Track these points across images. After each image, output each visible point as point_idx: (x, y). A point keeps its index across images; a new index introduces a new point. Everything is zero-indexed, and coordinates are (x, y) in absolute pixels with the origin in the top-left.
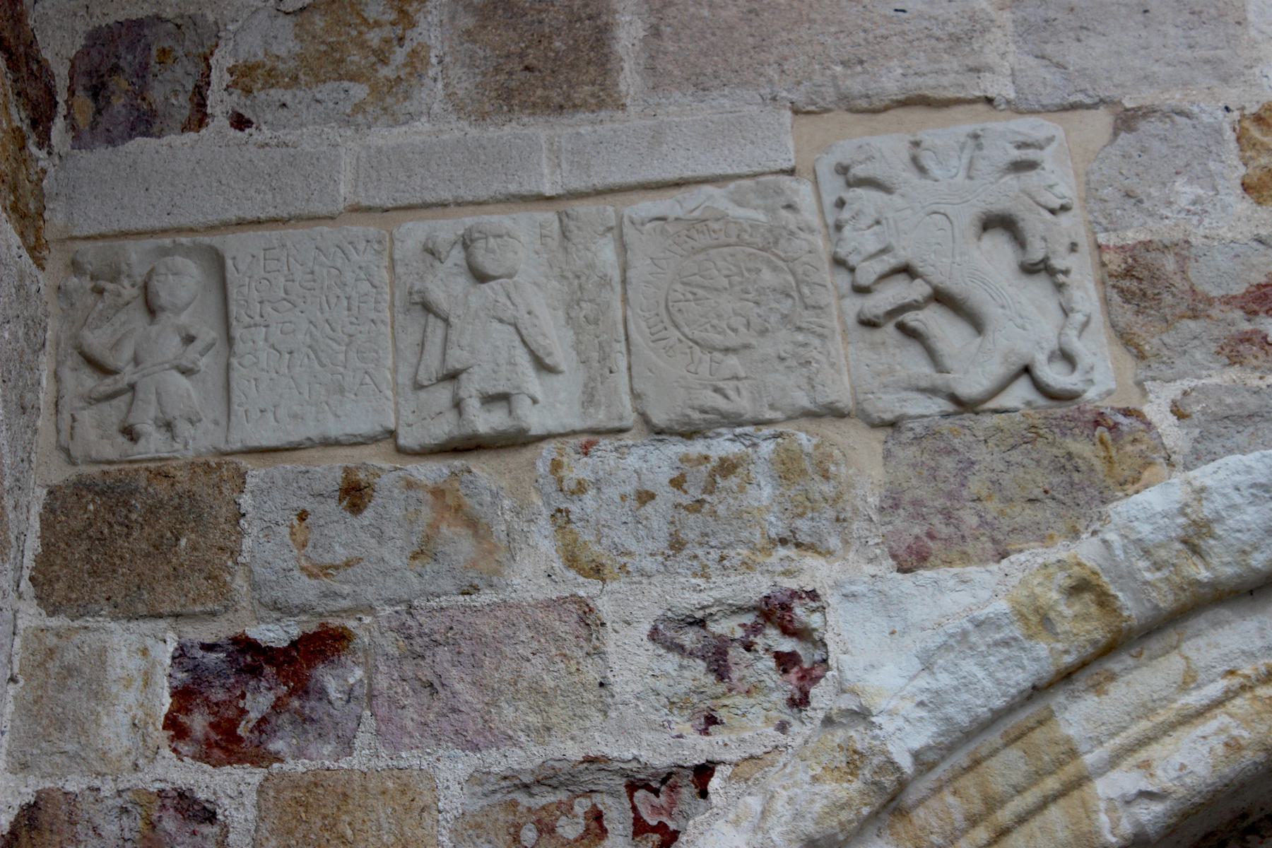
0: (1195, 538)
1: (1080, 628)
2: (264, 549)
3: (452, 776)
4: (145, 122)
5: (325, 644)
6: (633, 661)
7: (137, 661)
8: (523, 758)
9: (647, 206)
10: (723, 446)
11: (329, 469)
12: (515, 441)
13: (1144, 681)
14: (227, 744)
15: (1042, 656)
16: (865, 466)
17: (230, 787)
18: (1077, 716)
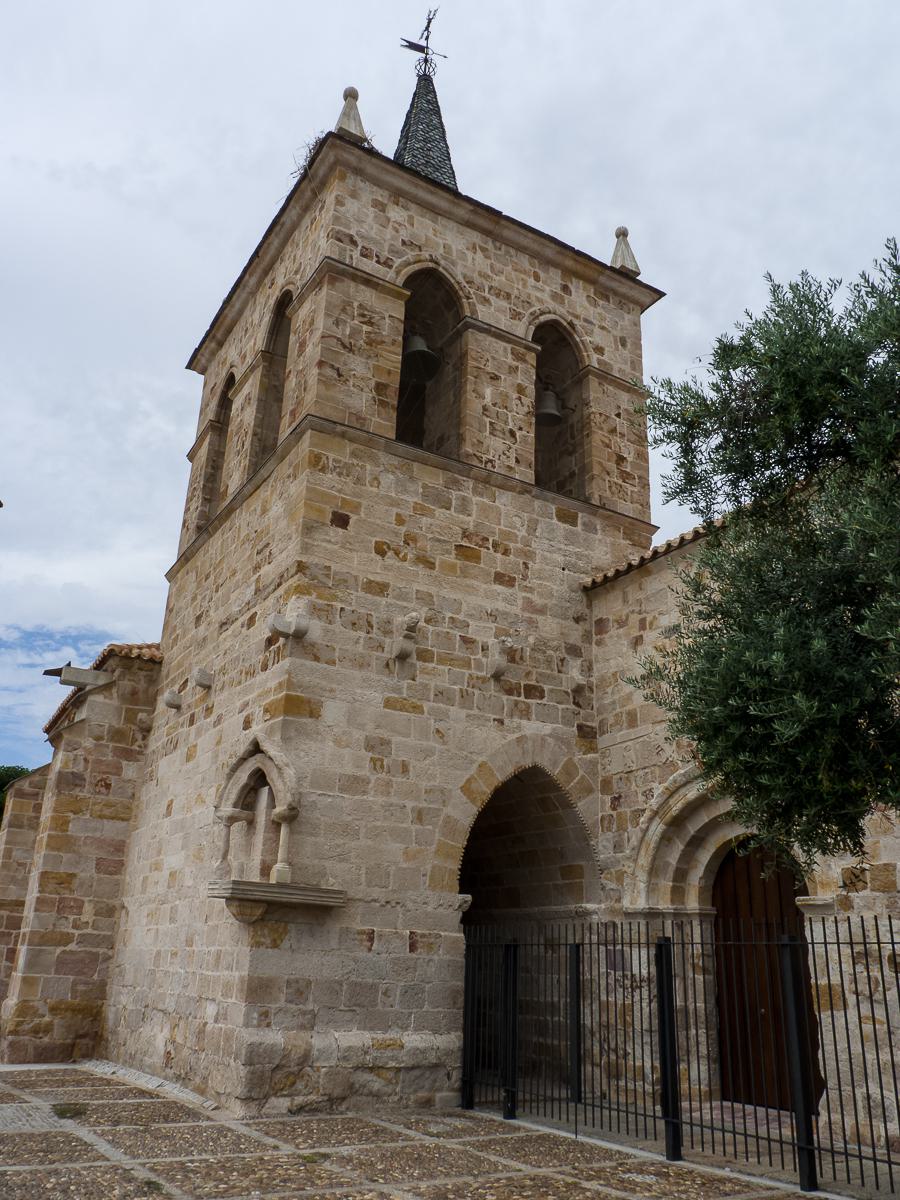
0: (675, 781)
1: (668, 792)
2: (615, 787)
3: (628, 810)
4: (604, 733)
5: (620, 796)
6: (641, 798)
7: (608, 799)
8: (633, 809)
9: (641, 739)
10: (646, 770)
11: (618, 776)
12: (632, 771)
13: (676, 796)
14: (614, 809)
15: (665, 797)
16: (657, 771)
17: (614, 813)
18: (672, 801)
